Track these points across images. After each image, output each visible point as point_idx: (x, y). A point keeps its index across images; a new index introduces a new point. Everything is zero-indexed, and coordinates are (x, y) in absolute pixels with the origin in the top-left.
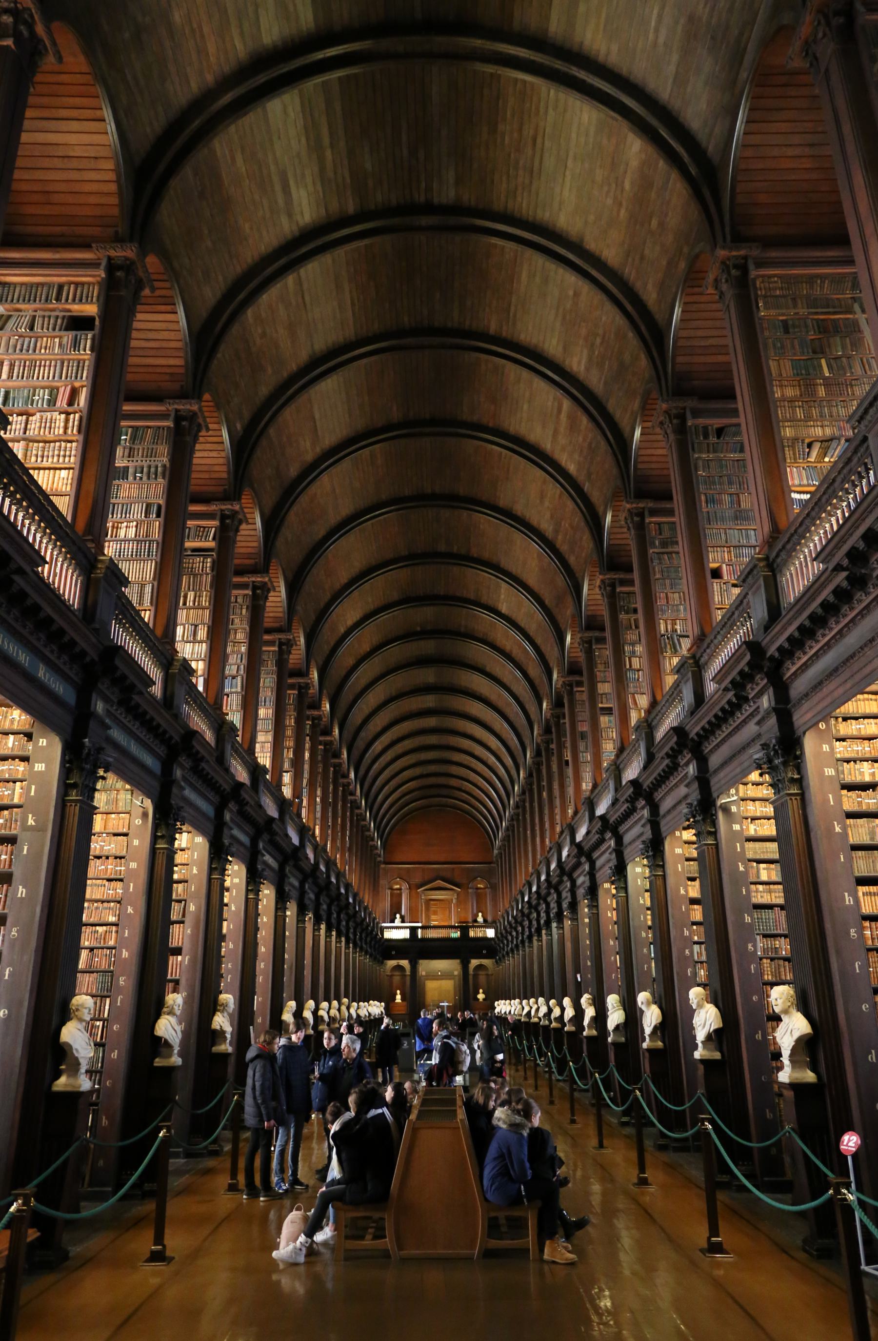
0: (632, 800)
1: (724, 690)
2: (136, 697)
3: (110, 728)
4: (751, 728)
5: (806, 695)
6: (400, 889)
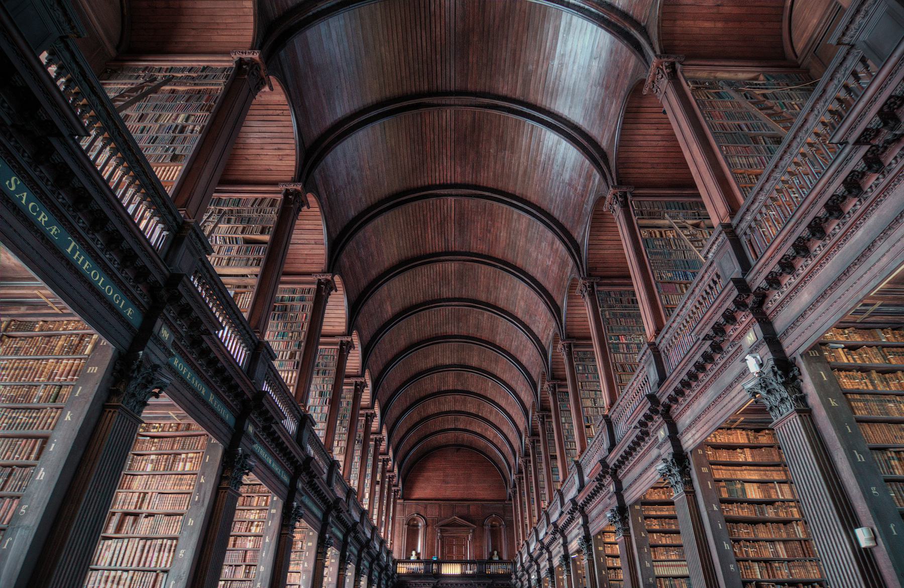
0: (571, 512)
1: (704, 339)
2: (274, 427)
3: (254, 443)
4: (655, 452)
5: (690, 426)
6: (417, 526)
